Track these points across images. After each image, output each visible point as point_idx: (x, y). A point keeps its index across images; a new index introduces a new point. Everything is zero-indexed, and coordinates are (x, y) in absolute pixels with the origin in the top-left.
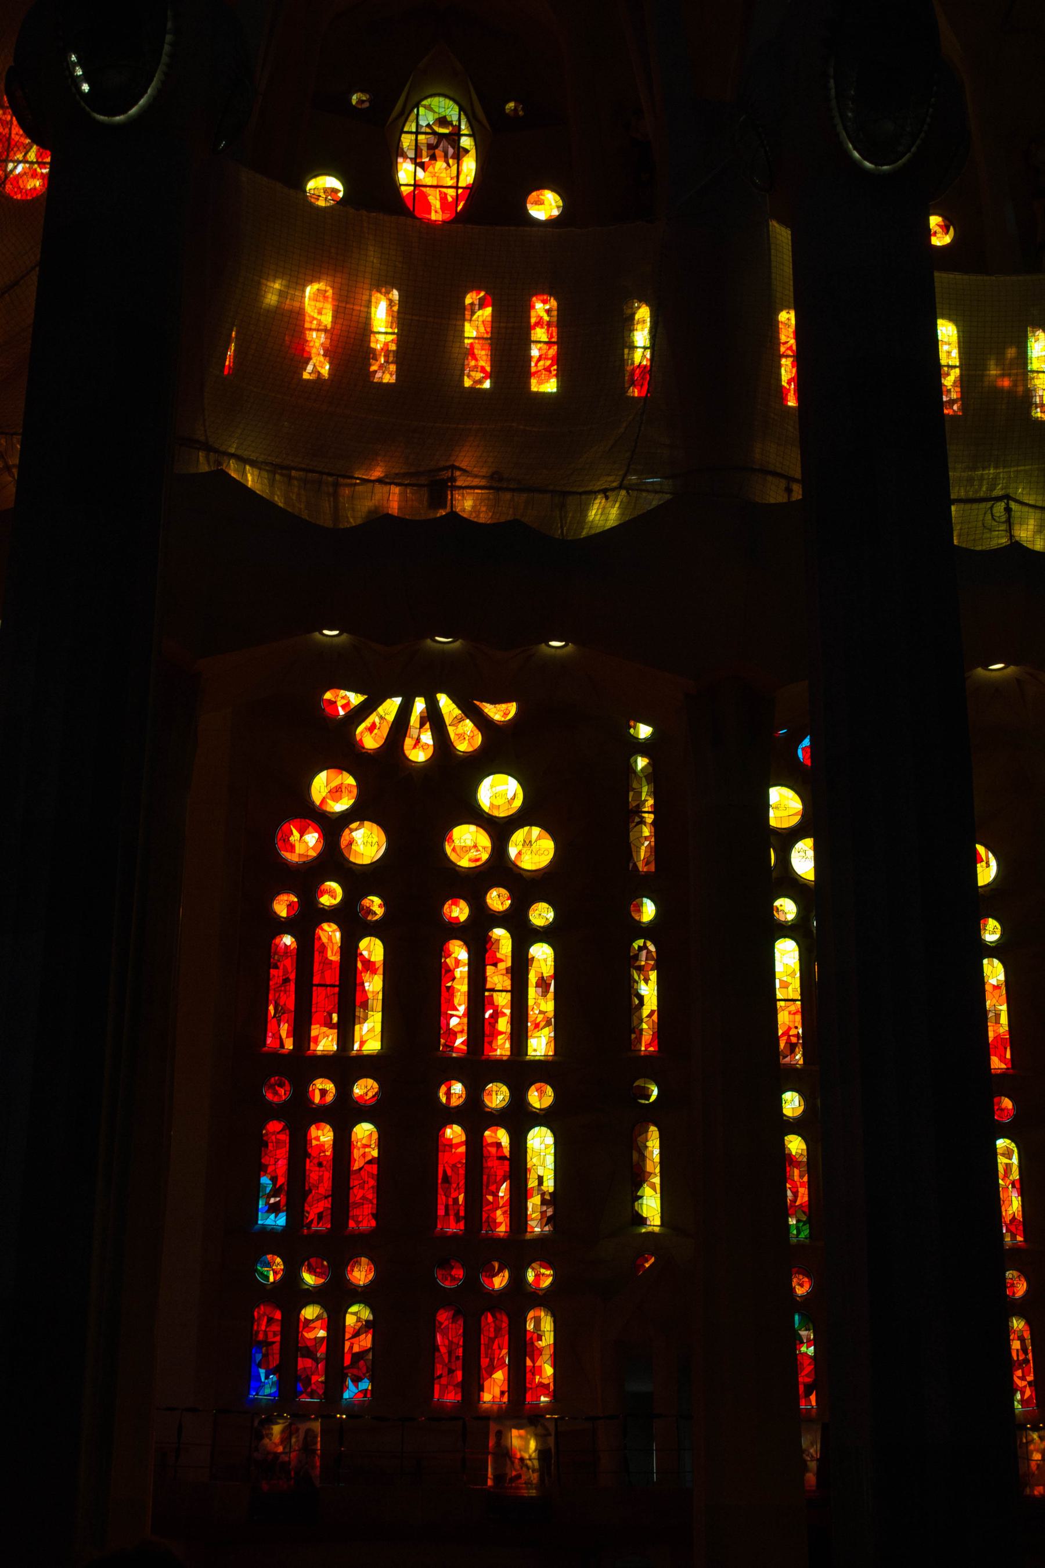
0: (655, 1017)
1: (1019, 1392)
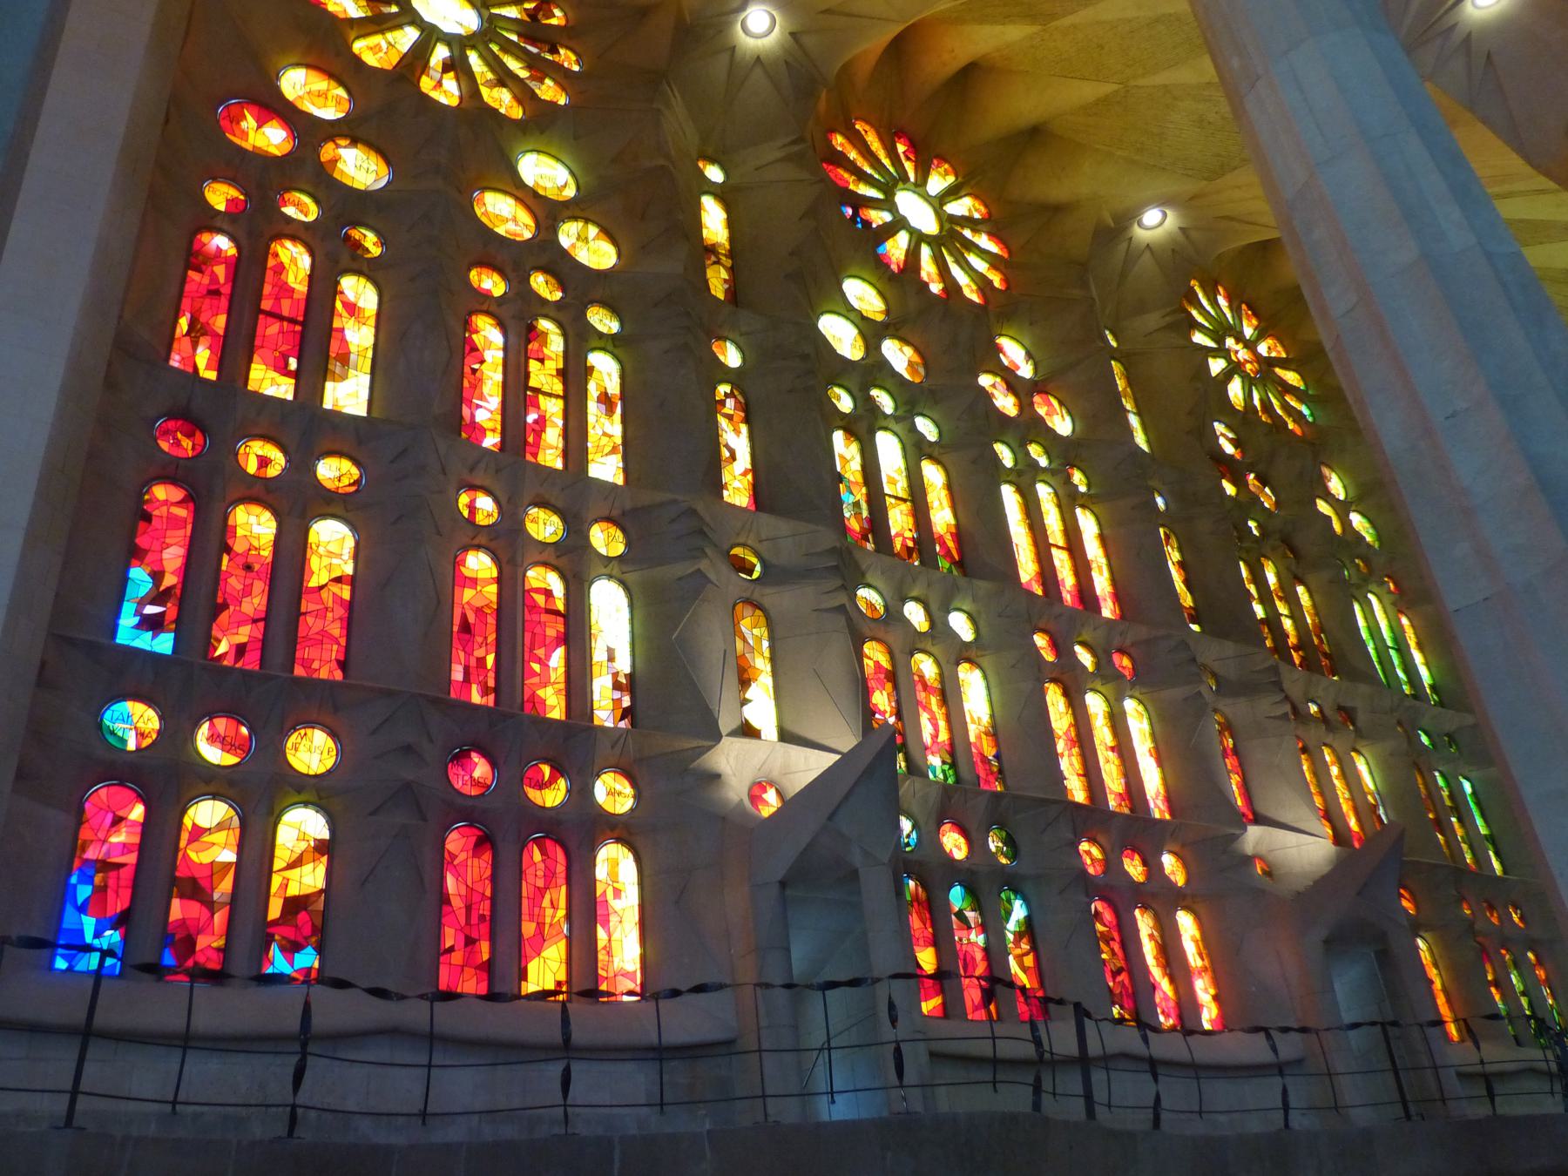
0: (750, 477)
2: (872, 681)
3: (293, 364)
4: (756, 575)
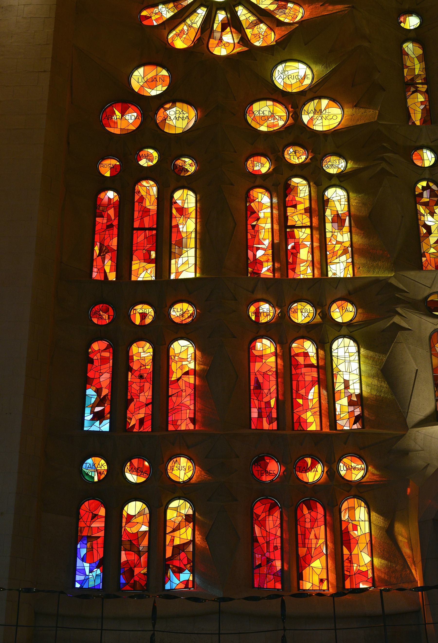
3: (153, 254)
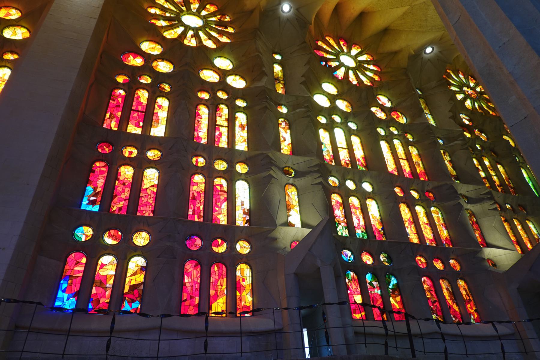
0: (291, 146)
1: (472, 315)
2: (335, 207)
3: (141, 124)
4: (293, 176)
